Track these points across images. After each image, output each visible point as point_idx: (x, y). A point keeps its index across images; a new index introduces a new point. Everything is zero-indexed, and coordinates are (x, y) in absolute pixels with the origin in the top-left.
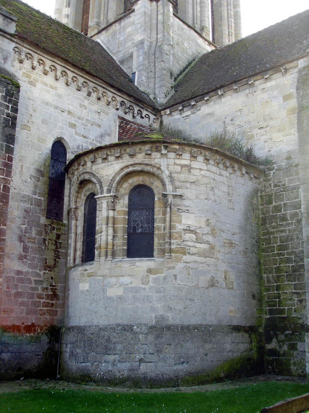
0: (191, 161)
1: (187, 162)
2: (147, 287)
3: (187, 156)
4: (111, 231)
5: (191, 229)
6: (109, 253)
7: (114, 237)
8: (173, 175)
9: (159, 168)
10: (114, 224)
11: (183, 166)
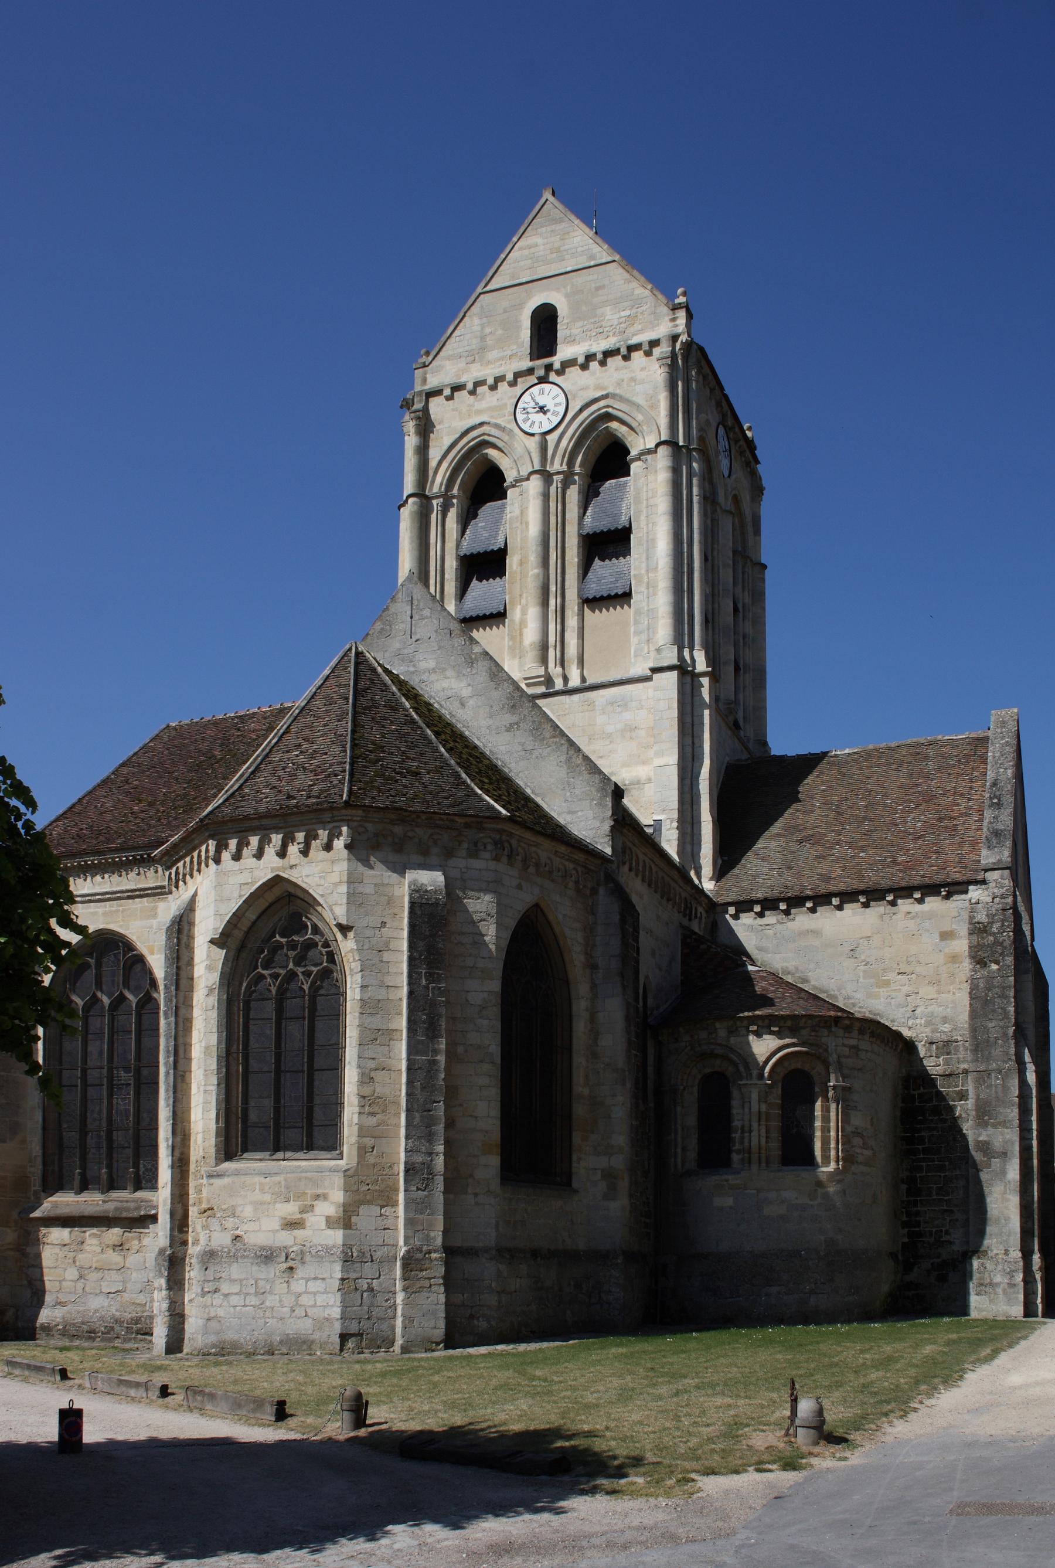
0: (859, 1039)
1: (853, 1042)
2: (815, 1203)
3: (855, 1033)
4: (763, 1132)
5: (859, 1131)
6: (763, 1160)
7: (767, 1137)
8: (843, 1060)
9: (826, 1050)
10: (767, 1120)
11: (851, 1047)
